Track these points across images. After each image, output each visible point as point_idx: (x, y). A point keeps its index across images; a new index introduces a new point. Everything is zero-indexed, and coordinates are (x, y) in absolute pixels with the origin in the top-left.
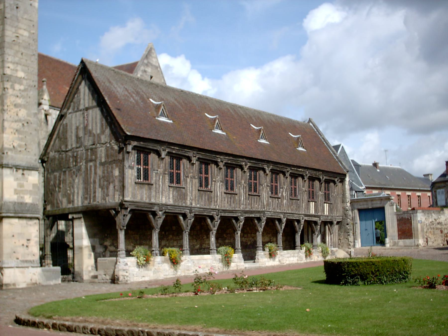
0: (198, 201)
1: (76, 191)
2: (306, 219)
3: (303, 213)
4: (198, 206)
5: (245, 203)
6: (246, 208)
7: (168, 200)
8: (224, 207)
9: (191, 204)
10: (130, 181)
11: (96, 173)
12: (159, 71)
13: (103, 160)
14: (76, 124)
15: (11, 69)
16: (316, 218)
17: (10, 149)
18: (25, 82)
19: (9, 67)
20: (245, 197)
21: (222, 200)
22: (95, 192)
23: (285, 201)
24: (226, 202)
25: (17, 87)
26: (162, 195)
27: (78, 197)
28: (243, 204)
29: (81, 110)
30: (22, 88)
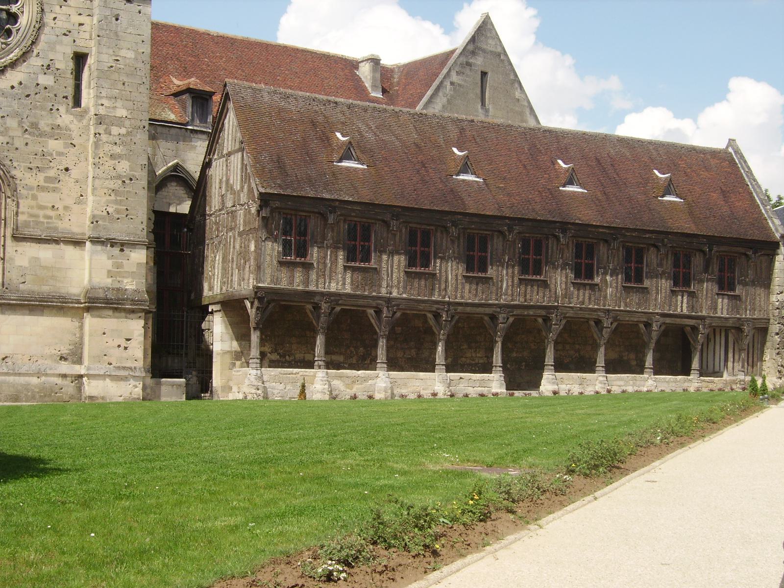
0: (405, 288)
1: (216, 273)
4: (404, 296)
5: (510, 292)
6: (512, 300)
7: (340, 287)
8: (462, 297)
9: (391, 293)
10: (268, 258)
11: (234, 247)
12: (502, 61)
13: (242, 229)
14: (219, 176)
15: (106, 107)
17: (103, 218)
18: (127, 123)
19: (102, 105)
20: (510, 283)
21: (457, 288)
22: (232, 276)
23: (609, 290)
24: (467, 291)
25: (115, 130)
26: (330, 279)
27: (217, 282)
28: (506, 294)
29: (224, 157)
30: (123, 131)
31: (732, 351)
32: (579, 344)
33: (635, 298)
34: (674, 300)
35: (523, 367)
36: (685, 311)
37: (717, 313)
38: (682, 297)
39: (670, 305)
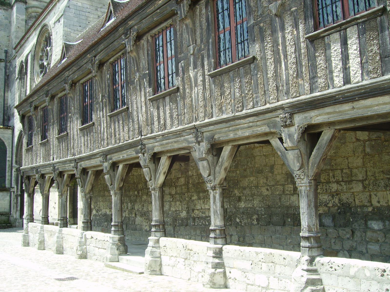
3: (285, 101)
32: (338, 182)
33: (234, 89)
34: (320, 61)
35: (255, 222)
36: (358, 79)
38: (344, 43)
39: (313, 78)
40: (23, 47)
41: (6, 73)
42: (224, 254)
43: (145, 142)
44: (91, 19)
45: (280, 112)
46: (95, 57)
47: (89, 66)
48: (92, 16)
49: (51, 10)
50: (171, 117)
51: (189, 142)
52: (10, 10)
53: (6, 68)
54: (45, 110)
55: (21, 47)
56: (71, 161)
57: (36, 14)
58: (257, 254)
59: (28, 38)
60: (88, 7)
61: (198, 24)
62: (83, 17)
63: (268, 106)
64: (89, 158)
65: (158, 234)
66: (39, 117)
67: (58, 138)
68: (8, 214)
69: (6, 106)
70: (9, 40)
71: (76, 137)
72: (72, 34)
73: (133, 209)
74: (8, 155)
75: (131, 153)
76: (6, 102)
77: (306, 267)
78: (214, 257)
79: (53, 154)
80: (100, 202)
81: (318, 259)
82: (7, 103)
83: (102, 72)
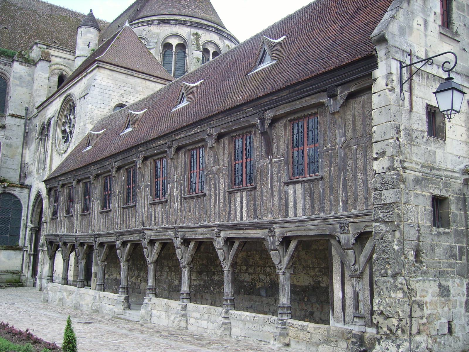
2: (231, 236)
3: (217, 223)
16: (260, 231)
31: (339, 278)
37: (287, 215)
40: (46, 109)
41: (25, 129)
42: (188, 309)
43: (146, 231)
44: (114, 97)
45: (215, 228)
46: (115, 162)
47: (110, 168)
48: (115, 94)
49: (76, 83)
50: (162, 218)
51: (172, 236)
52: (33, 67)
53: (25, 125)
54: (71, 189)
55: (43, 109)
56: (91, 235)
57: (58, 71)
58: (204, 308)
59: (51, 102)
60: (112, 85)
61: (180, 163)
62: (107, 96)
63: (210, 223)
64: (107, 235)
65: (151, 295)
66: (65, 194)
67: (81, 216)
68: (19, 273)
69: (23, 163)
70: (31, 97)
71: (96, 217)
72: (96, 111)
73: (139, 275)
74: (23, 214)
75: (136, 237)
76: (23, 159)
77: (223, 316)
78: (181, 310)
79: (77, 227)
80: (112, 267)
81: (230, 311)
82: (25, 161)
83: (119, 174)
